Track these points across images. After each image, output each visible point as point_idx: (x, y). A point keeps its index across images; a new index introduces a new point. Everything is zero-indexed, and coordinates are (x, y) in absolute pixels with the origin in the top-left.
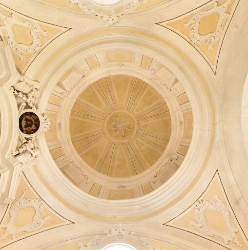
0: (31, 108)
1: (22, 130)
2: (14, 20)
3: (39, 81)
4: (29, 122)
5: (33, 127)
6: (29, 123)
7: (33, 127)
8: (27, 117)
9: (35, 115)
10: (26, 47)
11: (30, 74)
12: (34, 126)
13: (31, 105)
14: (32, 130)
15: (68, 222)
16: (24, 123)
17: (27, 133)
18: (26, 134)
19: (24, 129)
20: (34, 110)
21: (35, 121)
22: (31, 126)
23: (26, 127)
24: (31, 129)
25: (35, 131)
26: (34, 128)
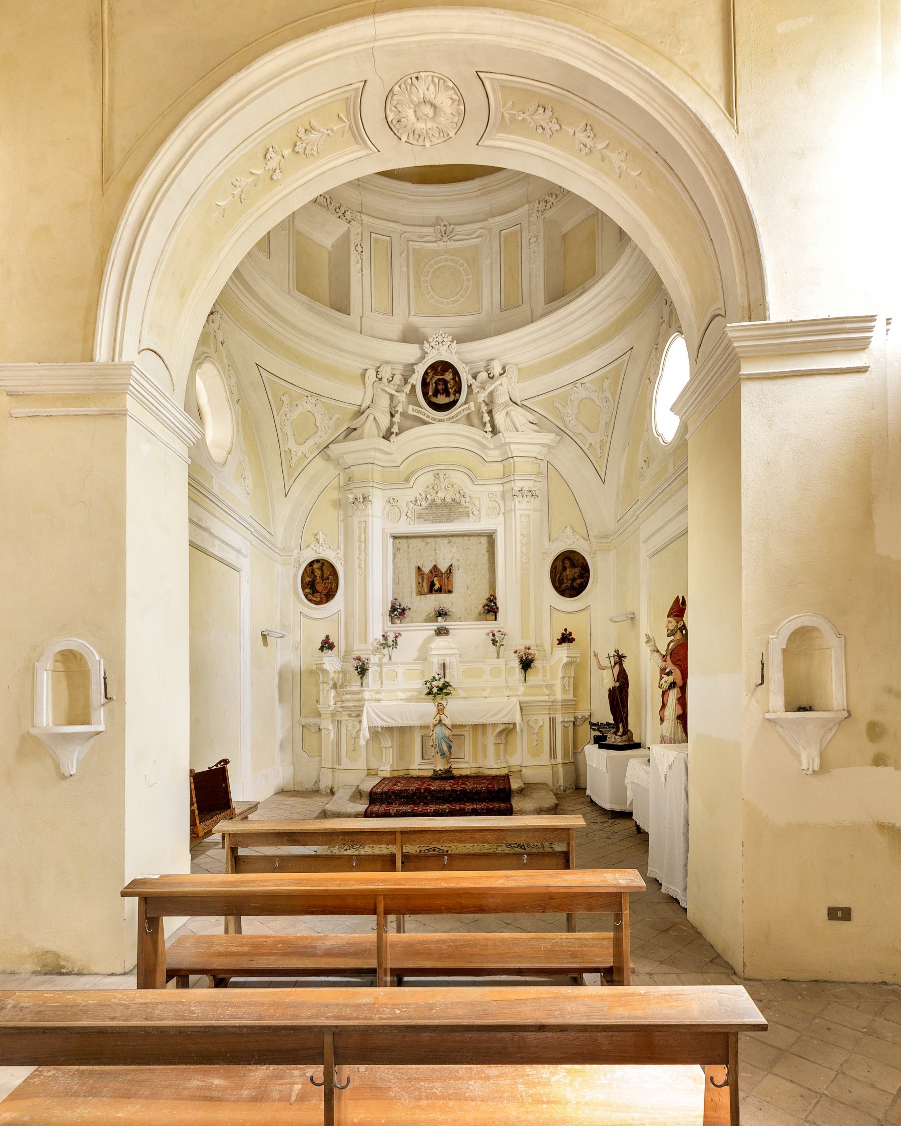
0: (413, 386)
1: (454, 403)
2: (291, 444)
3: (360, 371)
4: (440, 387)
5: (448, 376)
6: (441, 387)
7: (448, 376)
8: (430, 393)
9: (426, 373)
10: (319, 418)
11: (355, 396)
12: (447, 374)
13: (408, 388)
14: (454, 379)
15: (626, 357)
16: (442, 399)
17: (459, 391)
18: (460, 393)
19: (452, 398)
20: (416, 379)
21: (436, 373)
22: (445, 382)
23: (448, 395)
24: (452, 382)
25: (456, 373)
26: (451, 376)
